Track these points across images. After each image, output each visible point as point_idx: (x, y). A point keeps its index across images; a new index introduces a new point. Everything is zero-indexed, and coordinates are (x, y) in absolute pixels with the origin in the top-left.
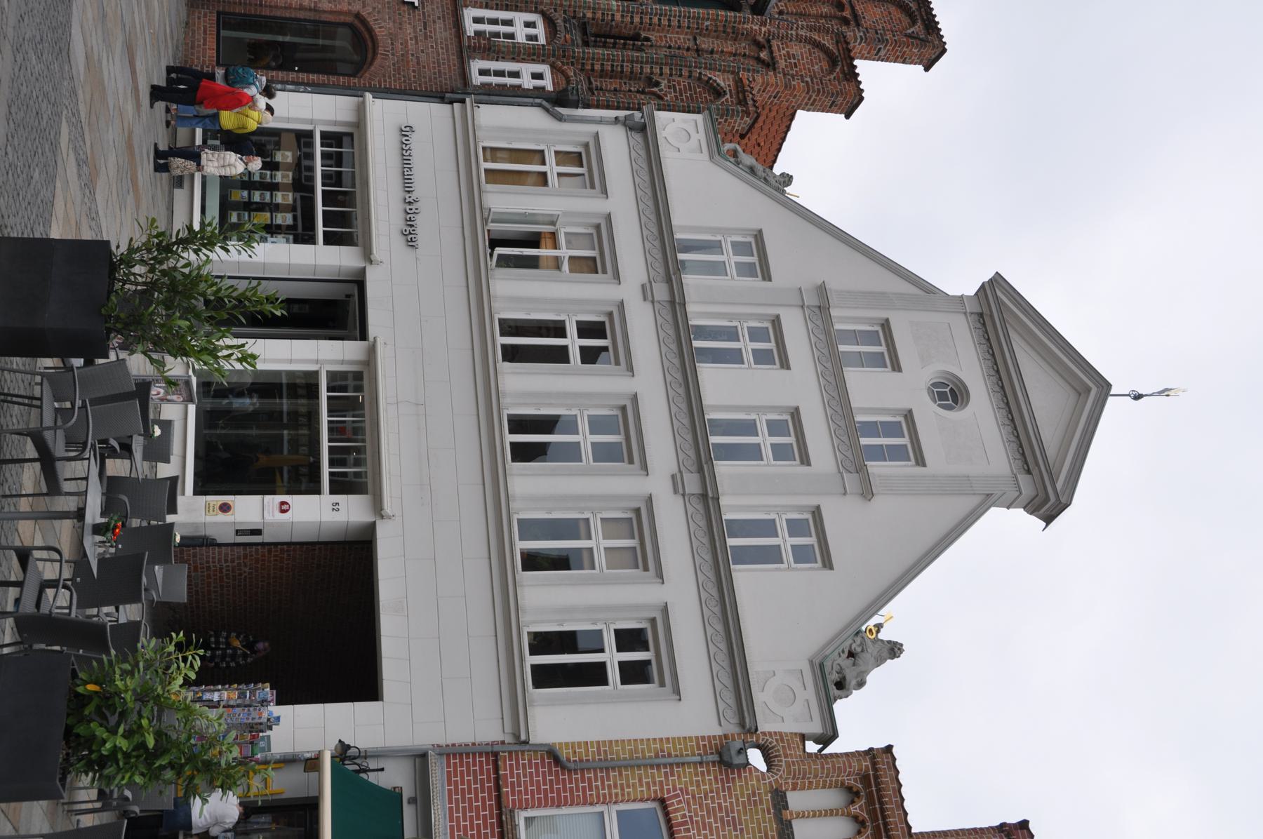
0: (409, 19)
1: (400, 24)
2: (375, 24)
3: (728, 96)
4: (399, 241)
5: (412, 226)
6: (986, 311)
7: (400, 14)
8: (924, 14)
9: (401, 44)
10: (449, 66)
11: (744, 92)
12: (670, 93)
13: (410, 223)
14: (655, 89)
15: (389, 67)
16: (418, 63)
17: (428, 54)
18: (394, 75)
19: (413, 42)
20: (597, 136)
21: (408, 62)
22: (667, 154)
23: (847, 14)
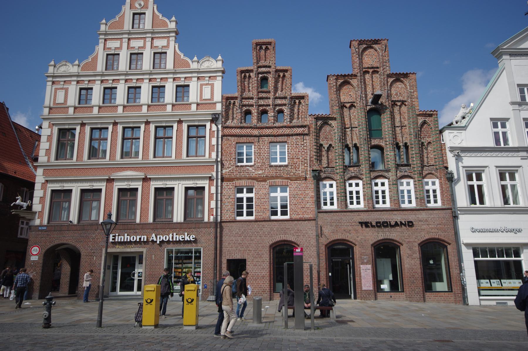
0: (419, 226)
1: (422, 229)
2: (424, 238)
3: (426, 120)
4: (519, 234)
5: (513, 230)
6: (510, 53)
7: (417, 230)
8: (369, 43)
10: (439, 214)
11: (426, 114)
12: (426, 139)
13: (511, 231)
14: (425, 144)
16: (440, 224)
17: (435, 221)
18: (448, 233)
19: (430, 225)
20: (463, 167)
21: (440, 228)
22: (464, 145)
23: (371, 71)
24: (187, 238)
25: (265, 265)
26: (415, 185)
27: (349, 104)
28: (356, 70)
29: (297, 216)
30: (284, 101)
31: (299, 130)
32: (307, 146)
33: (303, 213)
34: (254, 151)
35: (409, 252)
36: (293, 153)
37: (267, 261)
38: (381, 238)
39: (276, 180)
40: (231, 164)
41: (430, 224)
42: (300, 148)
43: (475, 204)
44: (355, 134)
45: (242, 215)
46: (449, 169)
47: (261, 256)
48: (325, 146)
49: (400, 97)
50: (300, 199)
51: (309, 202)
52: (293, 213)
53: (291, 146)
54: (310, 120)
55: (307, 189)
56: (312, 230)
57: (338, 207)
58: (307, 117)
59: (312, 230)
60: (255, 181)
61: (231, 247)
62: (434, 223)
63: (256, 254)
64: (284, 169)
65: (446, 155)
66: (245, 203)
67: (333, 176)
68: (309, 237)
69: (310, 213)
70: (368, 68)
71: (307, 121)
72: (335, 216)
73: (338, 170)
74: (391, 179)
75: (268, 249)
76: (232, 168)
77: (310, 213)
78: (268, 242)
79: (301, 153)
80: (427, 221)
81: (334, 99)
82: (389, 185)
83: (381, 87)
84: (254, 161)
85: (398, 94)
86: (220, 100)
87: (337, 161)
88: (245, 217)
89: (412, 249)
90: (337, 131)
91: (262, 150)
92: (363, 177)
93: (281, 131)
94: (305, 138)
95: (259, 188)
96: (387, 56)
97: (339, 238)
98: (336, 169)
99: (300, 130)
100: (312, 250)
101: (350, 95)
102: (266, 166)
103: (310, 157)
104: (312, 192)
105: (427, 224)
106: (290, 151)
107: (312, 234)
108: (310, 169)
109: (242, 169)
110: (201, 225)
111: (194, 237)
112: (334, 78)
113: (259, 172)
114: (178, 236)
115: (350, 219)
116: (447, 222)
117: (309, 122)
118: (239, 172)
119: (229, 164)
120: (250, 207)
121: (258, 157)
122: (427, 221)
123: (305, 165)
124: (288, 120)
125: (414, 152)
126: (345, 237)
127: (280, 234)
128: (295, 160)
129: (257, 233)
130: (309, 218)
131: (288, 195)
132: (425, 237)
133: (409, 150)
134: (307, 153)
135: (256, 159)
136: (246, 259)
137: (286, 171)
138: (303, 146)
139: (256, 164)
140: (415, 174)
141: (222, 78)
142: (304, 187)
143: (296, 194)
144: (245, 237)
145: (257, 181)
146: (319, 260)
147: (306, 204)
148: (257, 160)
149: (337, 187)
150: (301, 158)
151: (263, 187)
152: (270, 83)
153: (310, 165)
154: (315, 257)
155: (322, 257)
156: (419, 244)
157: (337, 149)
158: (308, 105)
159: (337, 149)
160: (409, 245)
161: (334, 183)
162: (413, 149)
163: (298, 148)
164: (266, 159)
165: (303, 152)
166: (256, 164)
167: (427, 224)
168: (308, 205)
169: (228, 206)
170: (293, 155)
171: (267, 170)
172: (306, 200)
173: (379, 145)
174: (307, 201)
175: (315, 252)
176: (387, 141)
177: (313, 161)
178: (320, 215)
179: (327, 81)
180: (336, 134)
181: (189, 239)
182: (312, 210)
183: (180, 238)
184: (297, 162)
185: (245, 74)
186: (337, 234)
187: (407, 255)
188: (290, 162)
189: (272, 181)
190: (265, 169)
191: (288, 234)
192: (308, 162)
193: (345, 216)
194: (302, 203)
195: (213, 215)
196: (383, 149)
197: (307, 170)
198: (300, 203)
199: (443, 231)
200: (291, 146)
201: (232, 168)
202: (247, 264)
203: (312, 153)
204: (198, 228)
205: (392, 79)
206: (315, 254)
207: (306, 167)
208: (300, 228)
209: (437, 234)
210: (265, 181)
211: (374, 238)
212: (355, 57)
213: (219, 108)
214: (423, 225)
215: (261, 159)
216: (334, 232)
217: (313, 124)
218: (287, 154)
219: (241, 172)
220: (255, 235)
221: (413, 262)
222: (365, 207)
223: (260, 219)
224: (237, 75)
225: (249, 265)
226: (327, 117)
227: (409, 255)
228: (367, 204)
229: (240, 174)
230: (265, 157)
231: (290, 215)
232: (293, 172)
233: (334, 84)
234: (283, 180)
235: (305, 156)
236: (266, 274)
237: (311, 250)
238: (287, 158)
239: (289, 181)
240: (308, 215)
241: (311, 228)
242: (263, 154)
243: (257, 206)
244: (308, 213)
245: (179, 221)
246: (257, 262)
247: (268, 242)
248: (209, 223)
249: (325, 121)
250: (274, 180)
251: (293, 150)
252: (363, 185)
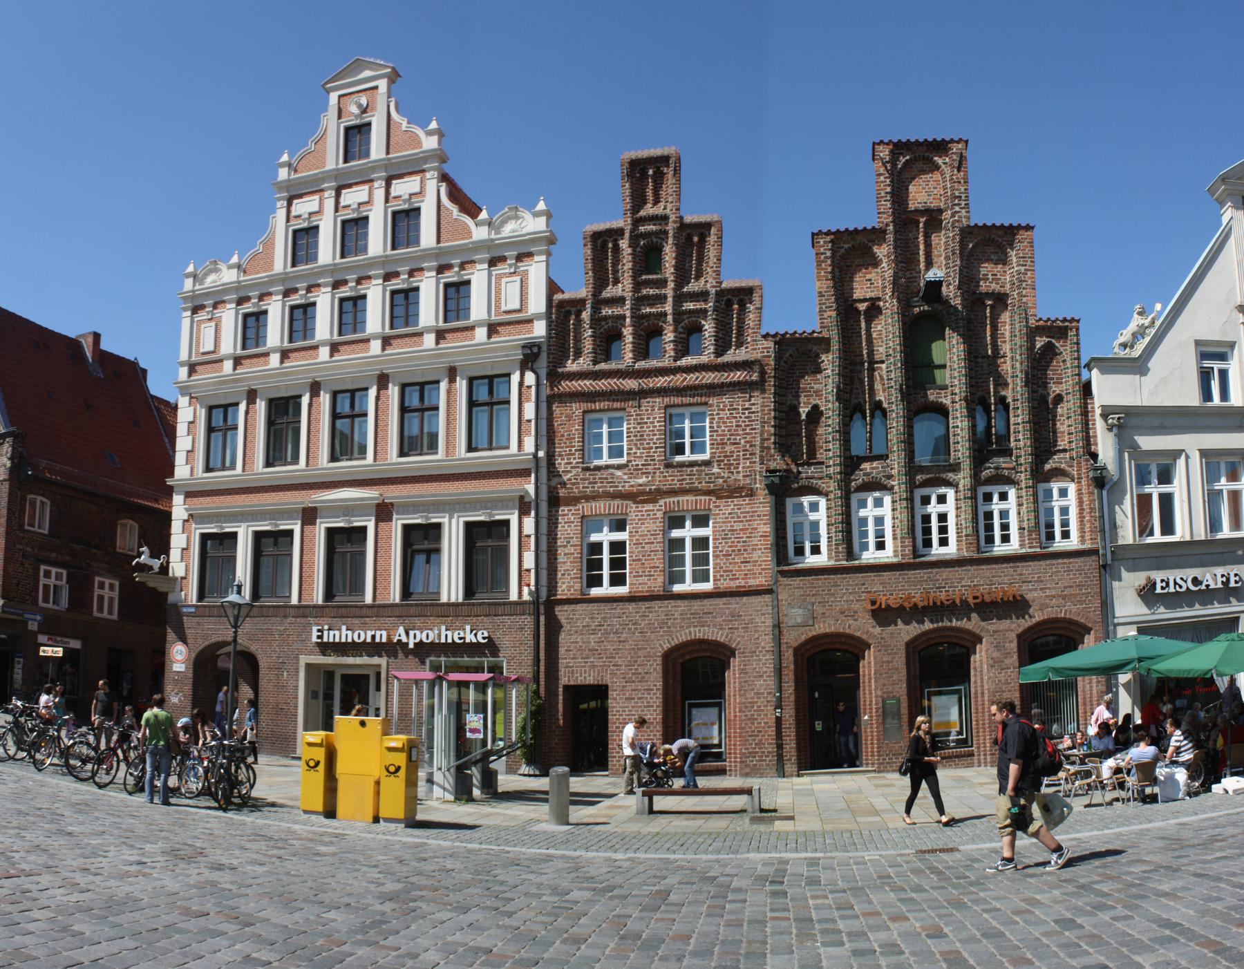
16: (1071, 587)
17: (1059, 580)
24: (470, 638)
25: (651, 698)
26: (1018, 497)
29: (732, 582)
30: (699, 305)
33: (746, 575)
34: (628, 429)
35: (996, 654)
36: (724, 431)
37: (658, 689)
39: (680, 499)
40: (571, 463)
41: (1049, 588)
43: (1151, 534)
44: (878, 378)
45: (600, 584)
46: (1100, 458)
47: (643, 678)
49: (993, 285)
50: (738, 542)
52: (722, 576)
53: (718, 414)
57: (830, 558)
60: (629, 502)
61: (573, 658)
63: (633, 674)
64: (701, 471)
65: (1094, 424)
66: (606, 556)
67: (820, 482)
68: (756, 631)
69: (760, 573)
73: (832, 469)
74: (961, 486)
75: (659, 661)
76: (574, 472)
77: (760, 573)
78: (660, 645)
79: (743, 430)
80: (1042, 581)
82: (957, 500)
83: (947, 258)
84: (628, 454)
85: (990, 277)
86: (542, 308)
87: (831, 447)
88: (605, 590)
90: (833, 371)
91: (648, 427)
92: (893, 483)
93: (692, 378)
95: (639, 520)
98: (827, 467)
99: (738, 376)
101: (870, 280)
102: (655, 464)
103: (763, 440)
104: (765, 524)
105: (1041, 589)
106: (715, 425)
109: (599, 474)
110: (500, 610)
111: (486, 635)
112: (828, 238)
113: (640, 481)
114: (449, 633)
118: (590, 483)
119: (567, 464)
120: (618, 564)
121: (636, 445)
122: (1042, 581)
124: (712, 349)
125: (1020, 420)
126: (844, 628)
127: (688, 627)
128: (728, 448)
129: (634, 624)
130: (758, 586)
131: (711, 533)
133: (1011, 415)
135: (631, 449)
136: (606, 687)
137: (706, 475)
139: (631, 461)
140: (1021, 472)
141: (549, 254)
142: (748, 512)
143: (729, 531)
144: (606, 633)
145: (636, 502)
146: (781, 682)
148: (634, 451)
149: (828, 509)
150: (742, 441)
151: (649, 515)
152: (667, 258)
154: (769, 676)
155: (787, 675)
156: (1019, 636)
157: (829, 417)
159: (829, 417)
161: (823, 503)
162: (1019, 411)
163: (736, 418)
164: (657, 448)
166: (631, 461)
167: (1041, 589)
168: (755, 556)
169: (565, 563)
170: (723, 435)
171: (658, 474)
173: (937, 402)
176: (956, 394)
177: (768, 448)
179: (813, 246)
180: (830, 380)
181: (474, 640)
183: (453, 636)
184: (733, 452)
185: (602, 242)
186: (824, 622)
187: (991, 662)
188: (715, 453)
189: (672, 499)
190: (654, 473)
191: (709, 626)
194: (745, 550)
195: (529, 585)
196: (948, 413)
198: (739, 550)
200: (718, 414)
201: (574, 472)
202: (610, 697)
204: (495, 616)
206: (769, 668)
208: (737, 610)
210: (654, 501)
213: (540, 329)
214: (1031, 590)
215: (644, 449)
217: (770, 357)
218: (708, 434)
219: (596, 483)
220: (630, 629)
221: (1002, 677)
222: (896, 556)
223: (642, 592)
224: (585, 245)
225: (615, 699)
226: (806, 337)
228: (900, 549)
229: (593, 487)
230: (654, 443)
231: (714, 580)
232: (723, 477)
233: (829, 254)
234: (698, 498)
236: (655, 719)
237: (760, 660)
238: (708, 443)
239: (714, 499)
240: (754, 578)
242: (648, 435)
243: (634, 560)
245: (453, 600)
246: (635, 690)
247: (660, 645)
248: (520, 603)
250: (676, 499)
251: (724, 423)
252: (893, 502)
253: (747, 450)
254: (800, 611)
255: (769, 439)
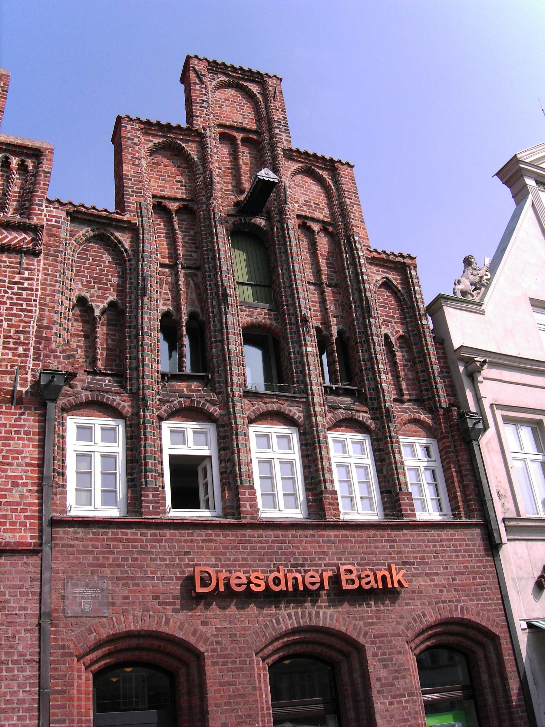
1: (414, 592)
9: (441, 591)
11: (388, 261)
15: (477, 605)
16: (462, 573)
23: (239, 136)
27: (177, 204)
28: (201, 122)
31: (10, 237)
32: (32, 290)
35: (383, 673)
38: (289, 624)
41: (437, 574)
42: (6, 292)
48: (94, 304)
51: (20, 481)
54: (49, 216)
55: (16, 432)
56: (27, 594)
58: (41, 205)
59: (27, 594)
62: (446, 568)
70: (231, 127)
71: (41, 215)
72: (120, 540)
77: (24, 524)
80: (427, 564)
81: (132, 176)
89: (391, 660)
94: (27, 264)
96: (280, 110)
97: (133, 628)
100: (21, 680)
103: (40, 327)
105: (427, 575)
107: (25, 609)
108: (34, 365)
115: (177, 553)
116: (479, 567)
117: (47, 220)
123: (16, 349)
126: (159, 623)
132: (424, 615)
134: (31, 311)
138: (19, 289)
147: (11, 491)
153: (34, 353)
158: (50, 173)
160: (379, 648)
165: (15, 308)
167: (427, 575)
168: (14, 496)
172: (9, 473)
174: (16, 477)
175: (32, 685)
178: (61, 535)
182: (28, 513)
192: (32, 342)
193: (160, 541)
197: (24, 367)
199: (473, 595)
203: (47, 313)
205: (295, 166)
207: (19, 355)
209: (456, 607)
211: (266, 626)
212: (198, 92)
216: (113, 604)
227: (382, 685)
235: (21, 321)
240: (12, 531)
241: (21, 587)
244: (13, 524)
249: (102, 231)
253: (10, 337)
254: (89, 593)
255: (50, 328)
